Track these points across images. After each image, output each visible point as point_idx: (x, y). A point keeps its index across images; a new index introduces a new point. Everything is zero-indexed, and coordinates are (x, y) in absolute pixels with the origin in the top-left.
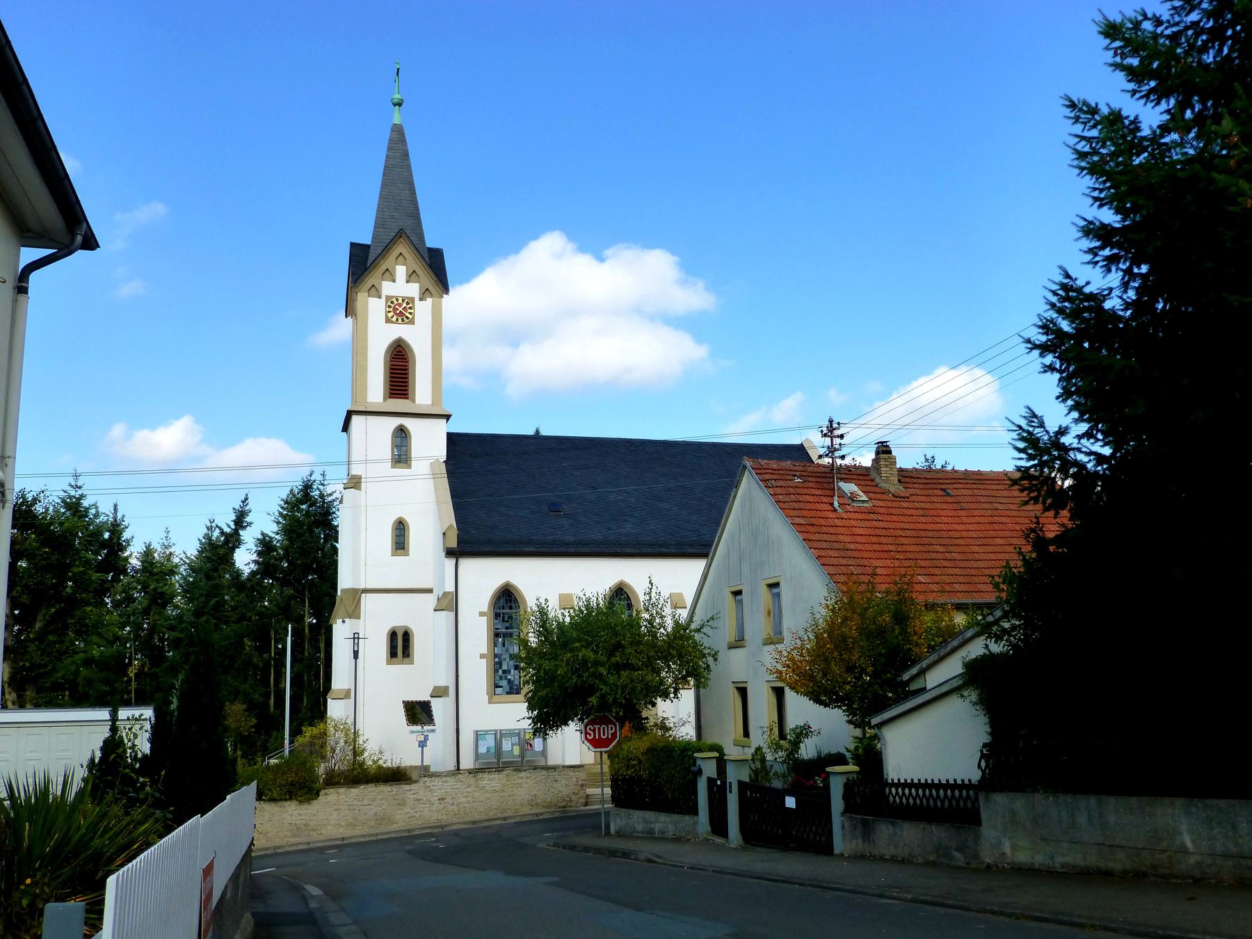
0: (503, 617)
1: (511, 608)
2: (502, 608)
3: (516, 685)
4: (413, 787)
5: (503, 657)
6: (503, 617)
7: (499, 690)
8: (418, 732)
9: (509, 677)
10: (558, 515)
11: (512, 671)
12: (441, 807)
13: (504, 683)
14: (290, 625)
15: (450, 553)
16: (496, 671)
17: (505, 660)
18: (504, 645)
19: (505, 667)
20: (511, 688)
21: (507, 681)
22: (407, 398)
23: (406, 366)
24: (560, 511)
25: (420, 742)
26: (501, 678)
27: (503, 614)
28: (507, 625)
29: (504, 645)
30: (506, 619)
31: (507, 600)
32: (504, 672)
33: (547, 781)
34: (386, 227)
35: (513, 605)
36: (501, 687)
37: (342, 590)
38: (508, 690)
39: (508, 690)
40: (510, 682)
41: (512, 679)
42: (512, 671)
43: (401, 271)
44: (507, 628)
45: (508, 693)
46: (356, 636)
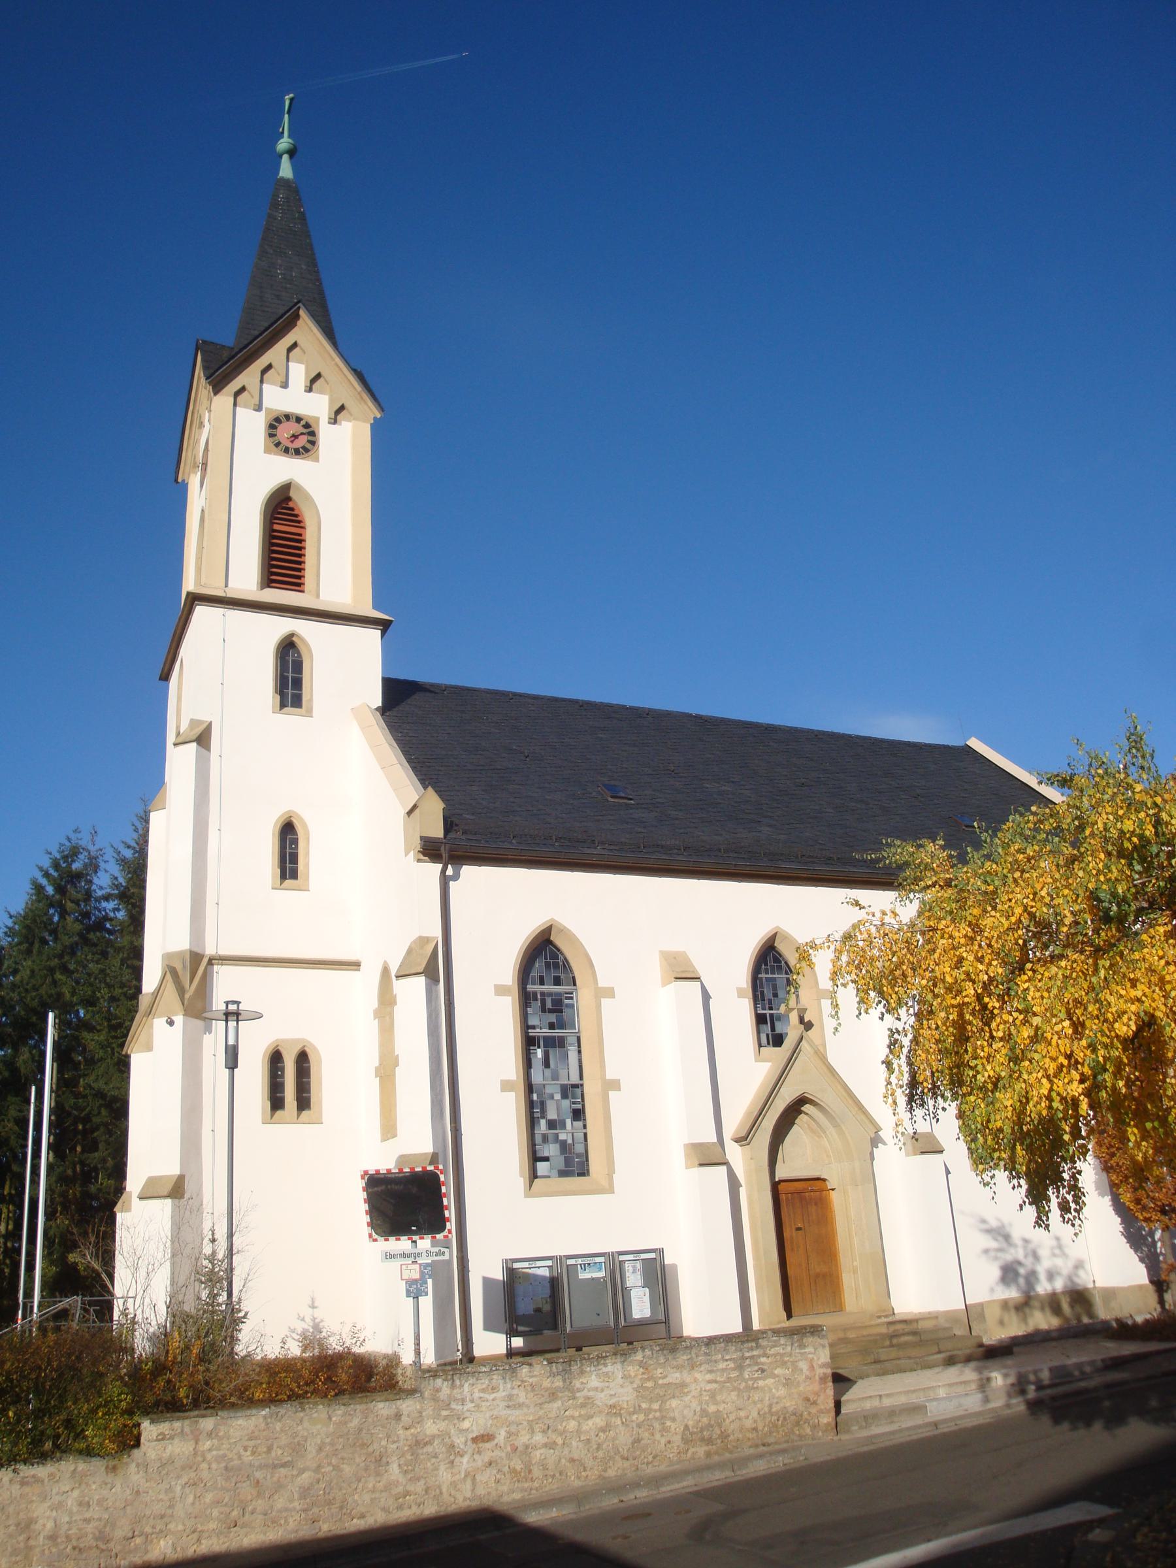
0: (543, 1002)
1: (557, 981)
2: (537, 980)
3: (578, 1156)
4: (407, 1406)
5: (548, 1090)
6: (543, 1002)
7: (542, 1167)
8: (404, 1255)
9: (562, 1137)
10: (627, 805)
11: (568, 1122)
12: (480, 1460)
13: (551, 1150)
14: (51, 1016)
15: (430, 850)
16: (532, 1123)
17: (552, 1097)
18: (547, 1064)
19: (552, 1115)
20: (568, 1162)
21: (558, 1146)
22: (303, 591)
23: (301, 535)
24: (631, 799)
25: (411, 1283)
26: (545, 1139)
27: (543, 994)
28: (553, 1018)
29: (547, 1064)
30: (549, 1005)
31: (548, 965)
32: (552, 1125)
33: (741, 1374)
34: (266, 309)
35: (562, 976)
36: (546, 1159)
37: (376, 606)
38: (562, 1167)
39: (562, 1167)
40: (564, 1146)
41: (570, 1141)
42: (568, 1122)
43: (298, 373)
44: (552, 1026)
45: (563, 1174)
46: (232, 1007)
